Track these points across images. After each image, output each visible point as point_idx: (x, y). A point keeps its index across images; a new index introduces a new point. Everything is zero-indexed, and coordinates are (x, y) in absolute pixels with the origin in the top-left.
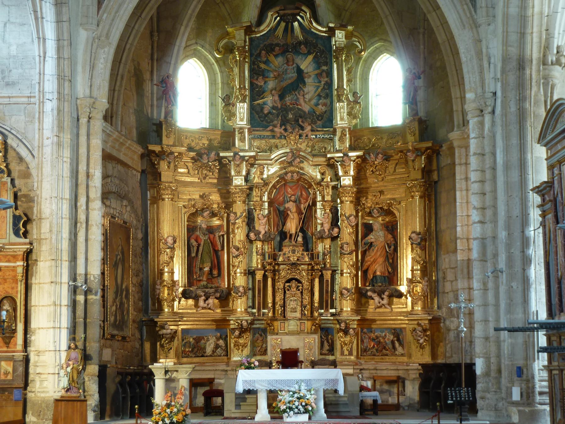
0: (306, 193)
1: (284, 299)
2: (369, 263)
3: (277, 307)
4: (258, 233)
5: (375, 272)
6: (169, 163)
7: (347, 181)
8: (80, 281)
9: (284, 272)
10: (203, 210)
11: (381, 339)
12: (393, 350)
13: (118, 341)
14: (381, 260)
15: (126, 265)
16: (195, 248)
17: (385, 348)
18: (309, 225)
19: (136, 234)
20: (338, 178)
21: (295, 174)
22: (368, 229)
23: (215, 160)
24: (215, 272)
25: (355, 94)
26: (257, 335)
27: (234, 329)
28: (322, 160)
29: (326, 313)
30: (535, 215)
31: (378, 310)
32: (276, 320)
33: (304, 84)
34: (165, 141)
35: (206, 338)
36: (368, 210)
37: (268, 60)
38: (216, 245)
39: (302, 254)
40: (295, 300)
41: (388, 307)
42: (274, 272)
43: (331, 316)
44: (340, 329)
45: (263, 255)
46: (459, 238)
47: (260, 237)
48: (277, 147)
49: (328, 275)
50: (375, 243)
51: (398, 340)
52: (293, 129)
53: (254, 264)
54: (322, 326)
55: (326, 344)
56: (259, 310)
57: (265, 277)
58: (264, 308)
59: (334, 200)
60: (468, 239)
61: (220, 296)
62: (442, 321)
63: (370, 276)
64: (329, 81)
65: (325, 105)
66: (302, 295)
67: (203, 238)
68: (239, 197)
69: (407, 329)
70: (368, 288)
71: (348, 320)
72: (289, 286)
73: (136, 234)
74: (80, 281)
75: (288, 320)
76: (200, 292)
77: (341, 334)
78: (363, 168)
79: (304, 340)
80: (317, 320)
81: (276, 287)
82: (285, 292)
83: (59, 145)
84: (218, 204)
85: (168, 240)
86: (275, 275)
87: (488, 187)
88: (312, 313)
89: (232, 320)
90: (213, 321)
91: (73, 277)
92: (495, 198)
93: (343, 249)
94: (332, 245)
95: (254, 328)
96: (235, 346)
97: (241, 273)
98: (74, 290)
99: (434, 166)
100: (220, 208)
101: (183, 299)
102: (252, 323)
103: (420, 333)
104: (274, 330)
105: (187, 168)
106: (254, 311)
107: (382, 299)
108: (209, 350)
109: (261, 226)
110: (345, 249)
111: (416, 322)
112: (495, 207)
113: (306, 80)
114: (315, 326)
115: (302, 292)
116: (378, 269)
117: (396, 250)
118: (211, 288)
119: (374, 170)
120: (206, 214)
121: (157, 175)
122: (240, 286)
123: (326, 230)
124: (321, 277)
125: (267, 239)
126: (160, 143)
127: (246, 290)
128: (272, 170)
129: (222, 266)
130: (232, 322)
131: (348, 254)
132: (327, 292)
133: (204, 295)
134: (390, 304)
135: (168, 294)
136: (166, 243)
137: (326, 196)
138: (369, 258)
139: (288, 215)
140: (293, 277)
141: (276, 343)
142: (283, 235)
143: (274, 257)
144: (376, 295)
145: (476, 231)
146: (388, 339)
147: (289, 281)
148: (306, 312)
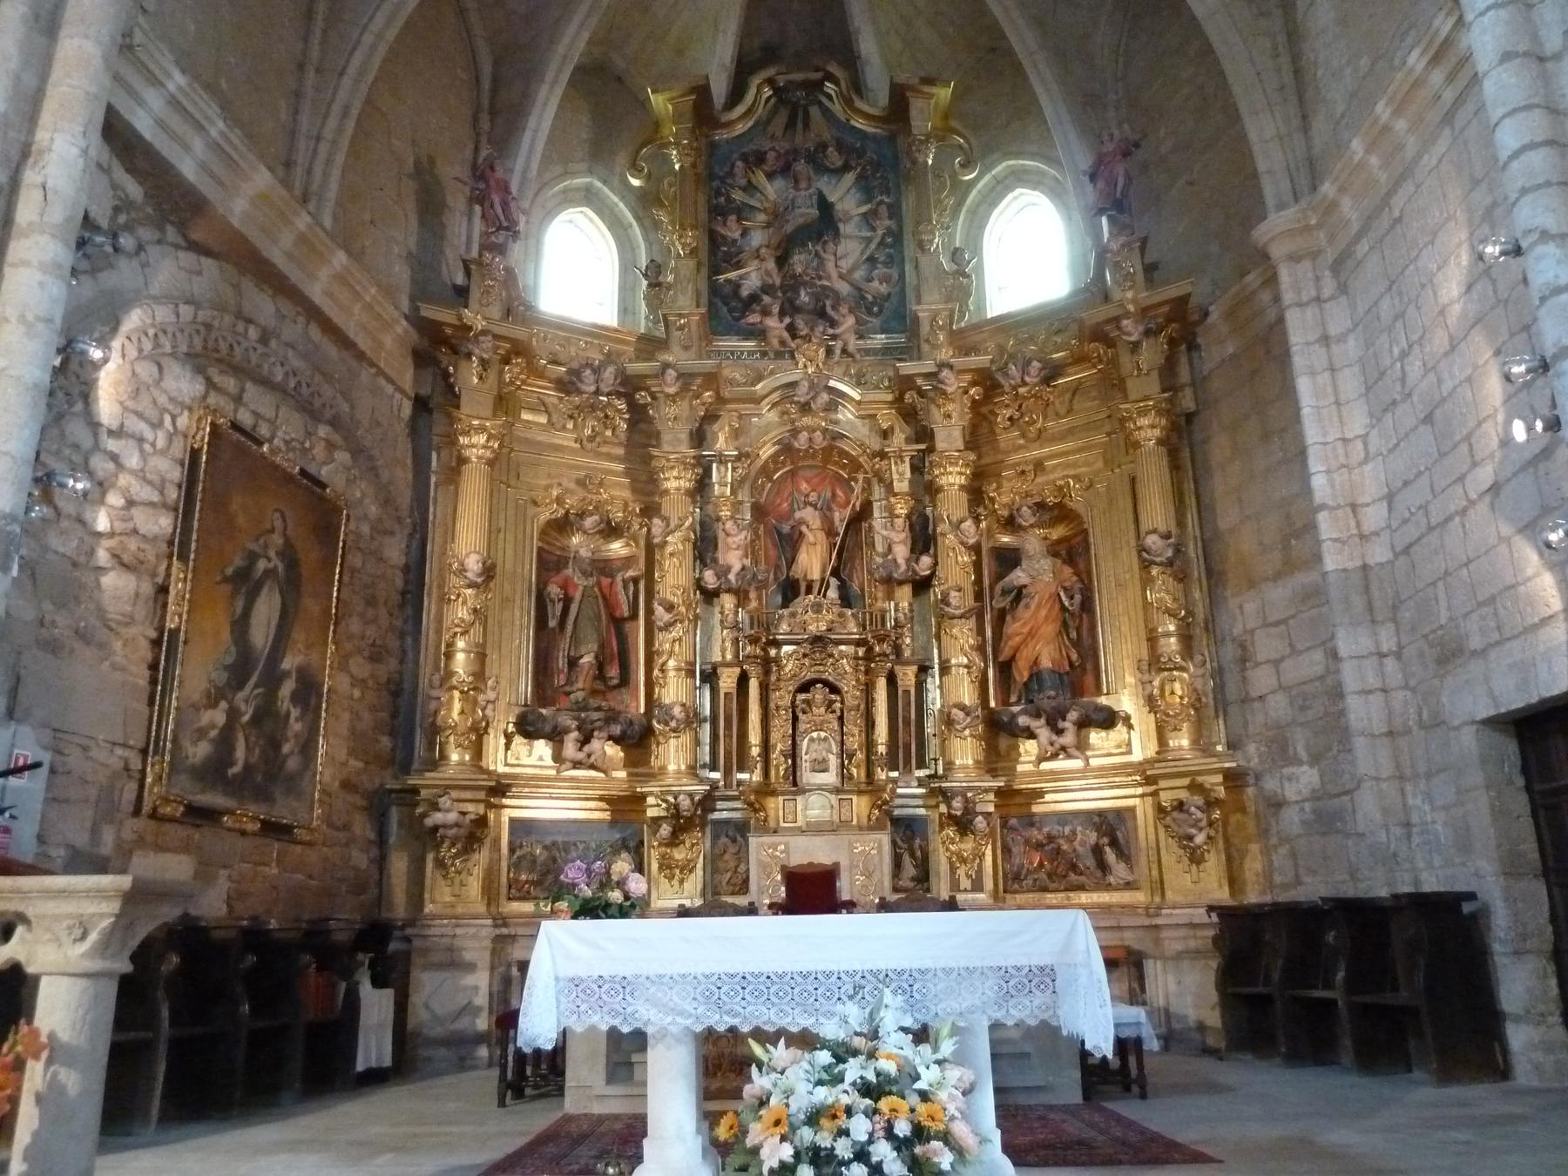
0: (845, 493)
1: (794, 737)
2: (1017, 639)
3: (775, 756)
4: (722, 573)
5: (1036, 662)
6: (484, 363)
11: (1062, 841)
12: (1099, 874)
13: (243, 833)
14: (1050, 629)
15: (310, 605)
16: (559, 607)
17: (1073, 867)
18: (853, 567)
21: (818, 433)
22: (1008, 559)
23: (619, 395)
24: (613, 672)
26: (724, 840)
27: (656, 821)
29: (907, 778)
31: (1045, 766)
32: (774, 793)
33: (837, 234)
35: (581, 847)
36: (1005, 513)
37: (749, 182)
38: (618, 605)
39: (841, 615)
40: (825, 739)
41: (1076, 753)
42: (767, 664)
43: (920, 786)
44: (950, 816)
45: (736, 626)
46: (1323, 507)
47: (728, 581)
49: (907, 676)
50: (1031, 589)
51: (1114, 843)
52: (812, 329)
53: (717, 657)
54: (897, 812)
55: (907, 859)
56: (728, 773)
57: (743, 680)
58: (741, 769)
60: (1354, 507)
61: (624, 733)
62: (1251, 780)
63: (1021, 673)
64: (894, 227)
65: (885, 279)
66: (842, 724)
67: (580, 582)
68: (676, 478)
69: (1139, 812)
70: (1015, 709)
71: (970, 789)
72: (807, 702)
75: (803, 792)
76: (567, 720)
77: (950, 832)
78: (984, 417)
79: (851, 847)
80: (884, 790)
81: (772, 705)
82: (795, 719)
84: (626, 505)
85: (467, 561)
86: (767, 672)
88: (870, 774)
89: (651, 794)
90: (601, 799)
93: (948, 604)
94: (915, 607)
95: (717, 822)
96: (660, 868)
97: (678, 669)
99: (1184, 375)
100: (630, 513)
101: (518, 740)
102: (707, 802)
103: (1199, 814)
104: (765, 820)
105: (546, 412)
106: (716, 775)
107: (1060, 732)
109: (733, 557)
110: (953, 602)
111: (1186, 781)
113: (841, 226)
114: (880, 807)
115: (841, 719)
116: (1046, 653)
117: (1087, 606)
118: (598, 709)
122: (674, 704)
124: (892, 680)
127: (692, 718)
129: (633, 659)
130: (651, 800)
131: (961, 617)
132: (907, 722)
133: (579, 729)
134: (1082, 746)
135: (462, 712)
138: (1013, 627)
139: (801, 534)
141: (773, 857)
142: (790, 590)
144: (1043, 721)
146: (1083, 843)
147: (805, 687)
148: (854, 771)
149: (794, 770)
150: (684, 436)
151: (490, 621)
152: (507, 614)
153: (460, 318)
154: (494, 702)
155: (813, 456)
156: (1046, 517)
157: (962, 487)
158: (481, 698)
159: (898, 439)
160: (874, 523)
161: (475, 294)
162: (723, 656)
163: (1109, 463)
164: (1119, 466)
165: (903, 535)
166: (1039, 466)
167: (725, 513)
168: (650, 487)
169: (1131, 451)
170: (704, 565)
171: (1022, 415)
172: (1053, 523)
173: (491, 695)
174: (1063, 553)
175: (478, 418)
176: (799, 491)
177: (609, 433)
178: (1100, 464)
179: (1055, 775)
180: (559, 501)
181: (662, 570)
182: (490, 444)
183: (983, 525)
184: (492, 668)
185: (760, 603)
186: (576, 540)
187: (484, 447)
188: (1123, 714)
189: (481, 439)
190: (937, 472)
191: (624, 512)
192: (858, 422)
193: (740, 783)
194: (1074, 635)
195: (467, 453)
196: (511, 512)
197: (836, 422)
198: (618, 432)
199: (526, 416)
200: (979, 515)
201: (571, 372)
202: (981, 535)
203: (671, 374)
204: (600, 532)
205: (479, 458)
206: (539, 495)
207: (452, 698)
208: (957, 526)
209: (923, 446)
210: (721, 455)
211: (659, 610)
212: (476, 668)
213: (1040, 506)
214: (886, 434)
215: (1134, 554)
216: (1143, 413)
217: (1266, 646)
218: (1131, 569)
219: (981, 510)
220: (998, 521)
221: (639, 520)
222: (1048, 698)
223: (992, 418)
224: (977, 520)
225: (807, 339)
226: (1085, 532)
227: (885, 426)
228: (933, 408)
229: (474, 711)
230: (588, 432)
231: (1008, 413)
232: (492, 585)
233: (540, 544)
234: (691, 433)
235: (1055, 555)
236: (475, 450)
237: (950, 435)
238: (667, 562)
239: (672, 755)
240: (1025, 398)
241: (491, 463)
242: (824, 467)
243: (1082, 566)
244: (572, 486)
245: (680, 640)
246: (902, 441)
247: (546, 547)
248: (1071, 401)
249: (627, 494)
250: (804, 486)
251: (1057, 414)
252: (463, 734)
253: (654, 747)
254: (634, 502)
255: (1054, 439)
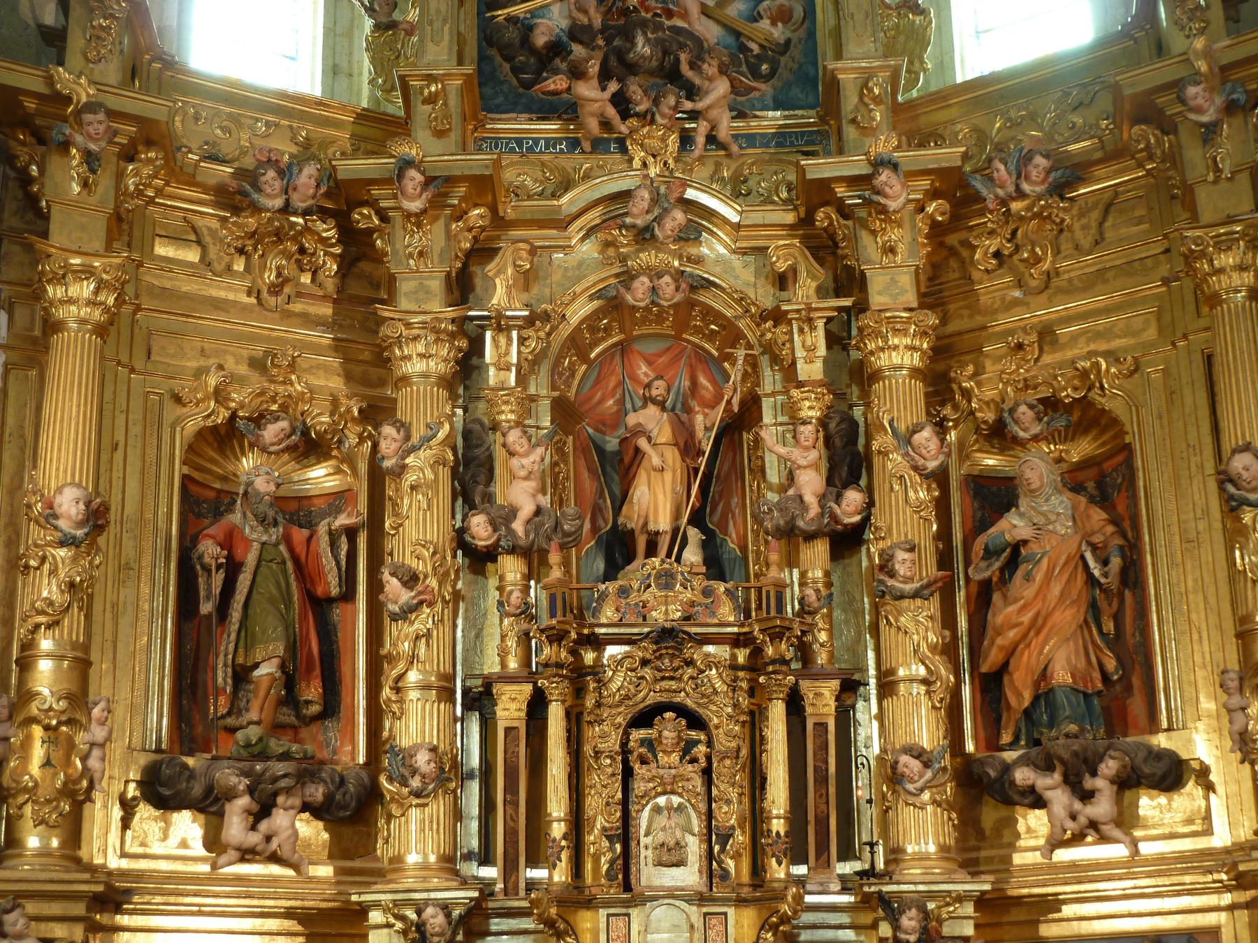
0: (713, 382)
1: (625, 803)
2: (1012, 634)
3: (594, 839)
5: (1044, 674)
6: (90, 159)
14: (1068, 617)
16: (218, 579)
18: (728, 510)
21: (667, 279)
23: (324, 213)
24: (312, 692)
29: (822, 877)
31: (1063, 855)
32: (590, 904)
36: (990, 416)
39: (707, 592)
40: (680, 808)
41: (1117, 833)
43: (844, 890)
45: (526, 612)
47: (511, 532)
50: (1034, 548)
52: (656, 102)
53: (491, 665)
56: (510, 869)
57: (537, 705)
58: (533, 862)
61: (329, 797)
63: (1019, 692)
66: (709, 783)
67: (255, 535)
68: (421, 356)
70: (1010, 756)
71: (932, 895)
72: (649, 744)
75: (640, 900)
76: (229, 776)
78: (953, 252)
80: (783, 898)
81: (588, 749)
82: (628, 773)
84: (335, 403)
85: (58, 500)
86: (579, 692)
88: (758, 870)
89: (376, 905)
90: (289, 914)
93: (892, 574)
94: (835, 578)
101: (145, 811)
105: (199, 242)
106: (489, 872)
107: (1087, 796)
110: (901, 570)
114: (774, 928)
115: (707, 773)
117: (1132, 575)
118: (285, 756)
119: (1008, 248)
122: (416, 748)
123: (810, 499)
129: (345, 669)
131: (915, 595)
132: (822, 779)
133: (251, 791)
134: (1126, 821)
135: (47, 763)
137: (800, 365)
139: (637, 450)
140: (663, 698)
144: (1057, 777)
147: (645, 718)
148: (730, 864)
150: (436, 284)
151: (98, 607)
152: (127, 593)
153: (50, 80)
154: (102, 746)
155: (660, 319)
156: (1060, 423)
157: (915, 372)
158: (81, 738)
159: (806, 289)
160: (763, 434)
161: (76, 42)
162: (503, 664)
163: (1169, 331)
164: (1185, 337)
165: (813, 455)
166: (1046, 335)
167: (507, 416)
168: (375, 372)
169: (1205, 310)
170: (470, 505)
171: (1017, 249)
172: (1071, 433)
173: (99, 733)
174: (1090, 485)
175: (79, 253)
176: (634, 379)
177: (306, 279)
178: (1151, 333)
179: (1078, 871)
180: (219, 395)
181: (396, 515)
182: (101, 298)
183: (952, 436)
184: (100, 685)
185: (567, 572)
186: (247, 463)
187: (91, 303)
188: (1195, 765)
189: (86, 289)
190: (871, 346)
191: (332, 415)
192: (736, 261)
193: (531, 885)
194: (1109, 626)
195: (60, 313)
196: (136, 415)
197: (699, 261)
198: (320, 274)
199: (163, 250)
200: (945, 419)
201: (240, 174)
202: (949, 455)
203: (414, 177)
204: (288, 449)
205: (82, 322)
206: (184, 386)
207: (28, 739)
208: (906, 439)
209: (847, 302)
210: (500, 316)
211: (392, 585)
212: (74, 688)
213: (1050, 405)
214: (782, 281)
215: (1212, 485)
216: (1222, 245)
218: (1207, 512)
219: (947, 411)
220: (977, 430)
221: (359, 429)
223: (965, 253)
224: (941, 428)
225: (647, 118)
226: (1128, 448)
227: (782, 266)
228: (865, 237)
229: (68, 762)
230: (270, 277)
231: (993, 244)
232: (101, 540)
233: (186, 470)
234: (449, 274)
235: (1077, 488)
236: (73, 308)
237: (894, 281)
238: (406, 501)
240: (1022, 218)
241: (101, 330)
242: (678, 337)
243: (1121, 508)
244: (243, 369)
245: (428, 635)
246: (812, 292)
247: (196, 475)
248: (1101, 224)
249: (336, 383)
250: (643, 370)
251: (1077, 247)
252: (48, 801)
253: (381, 822)
254: (349, 398)
255: (1071, 291)
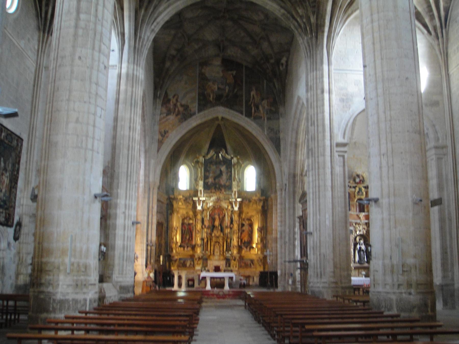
7: (236, 209)
8: (149, 242)
9: (214, 239)
10: (187, 217)
19: (165, 225)
20: (232, 207)
22: (243, 225)
25: (239, 179)
28: (228, 201)
30: (297, 225)
33: (222, 175)
34: (175, 194)
42: (211, 240)
48: (212, 196)
49: (229, 241)
57: (207, 241)
59: (231, 215)
63: (243, 241)
67: (186, 227)
73: (165, 225)
74: (149, 242)
83: (144, 198)
87: (283, 214)
91: (147, 241)
92: (285, 218)
98: (147, 245)
99: (266, 204)
108: (188, 265)
109: (207, 223)
112: (285, 221)
116: (246, 239)
120: (188, 219)
121: (172, 206)
123: (229, 226)
124: (227, 242)
125: (208, 228)
126: (173, 194)
128: (211, 204)
134: (250, 250)
136: (175, 228)
138: (243, 236)
142: (214, 226)
143: (211, 234)
145: (279, 229)
149: (214, 254)
217: (270, 242)
222: (246, 245)
239: (199, 251)
